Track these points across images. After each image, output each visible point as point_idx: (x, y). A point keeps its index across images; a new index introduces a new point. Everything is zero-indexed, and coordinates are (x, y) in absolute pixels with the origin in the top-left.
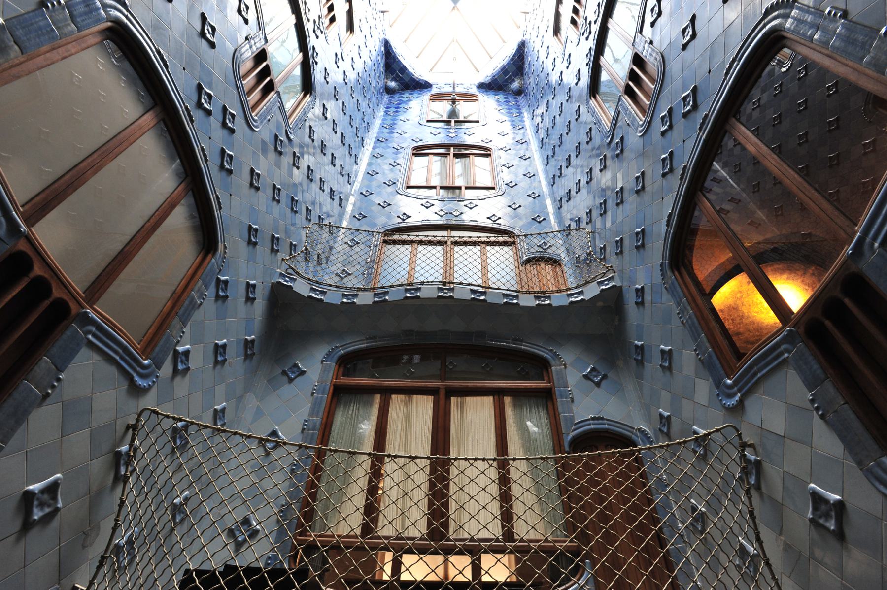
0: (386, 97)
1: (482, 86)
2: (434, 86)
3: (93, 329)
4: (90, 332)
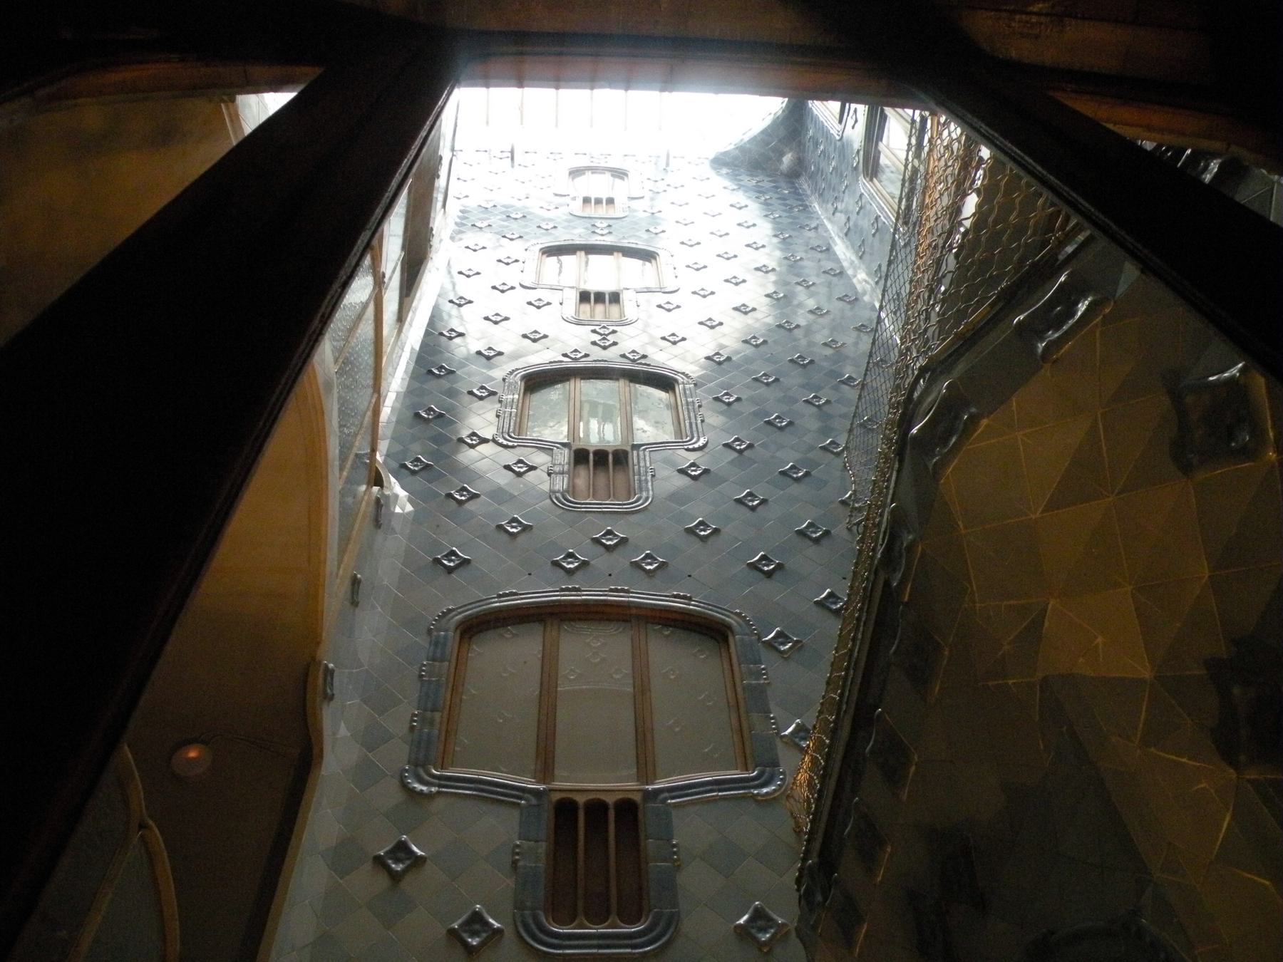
0: (804, 184)
3: (667, 794)
4: (666, 799)
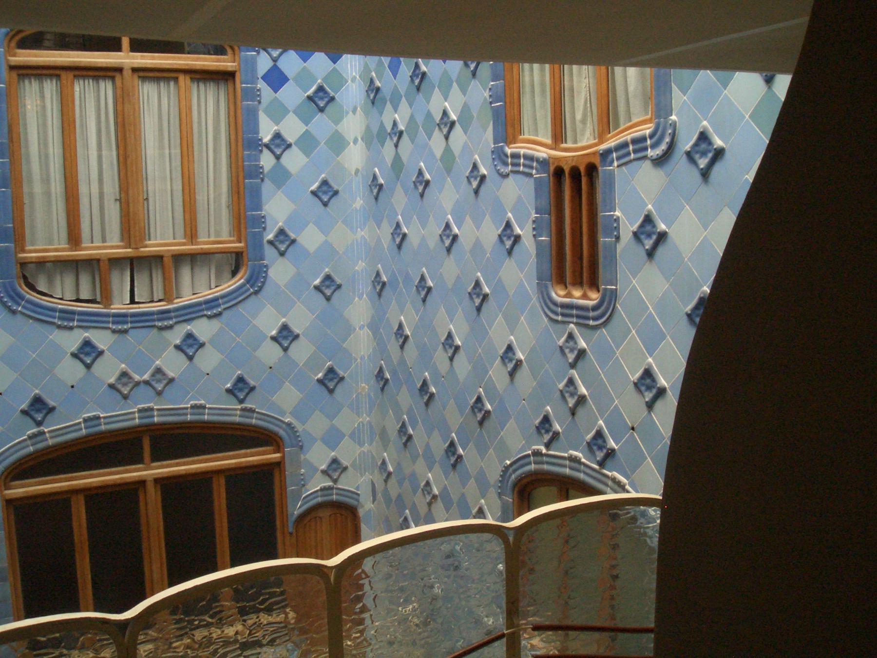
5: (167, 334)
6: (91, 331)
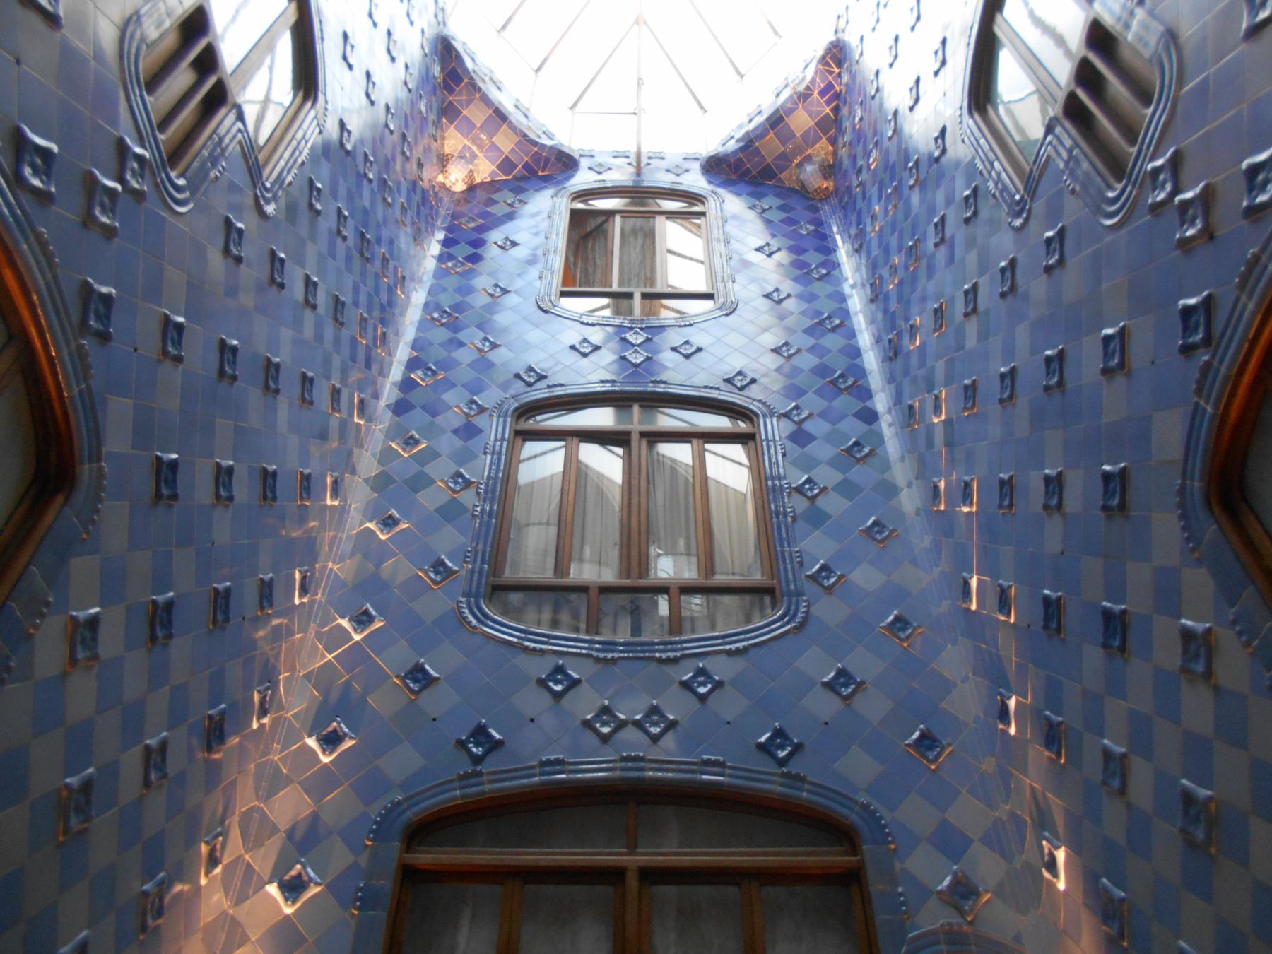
1: (717, 167)
2: (584, 163)
5: (669, 669)
6: (566, 657)
